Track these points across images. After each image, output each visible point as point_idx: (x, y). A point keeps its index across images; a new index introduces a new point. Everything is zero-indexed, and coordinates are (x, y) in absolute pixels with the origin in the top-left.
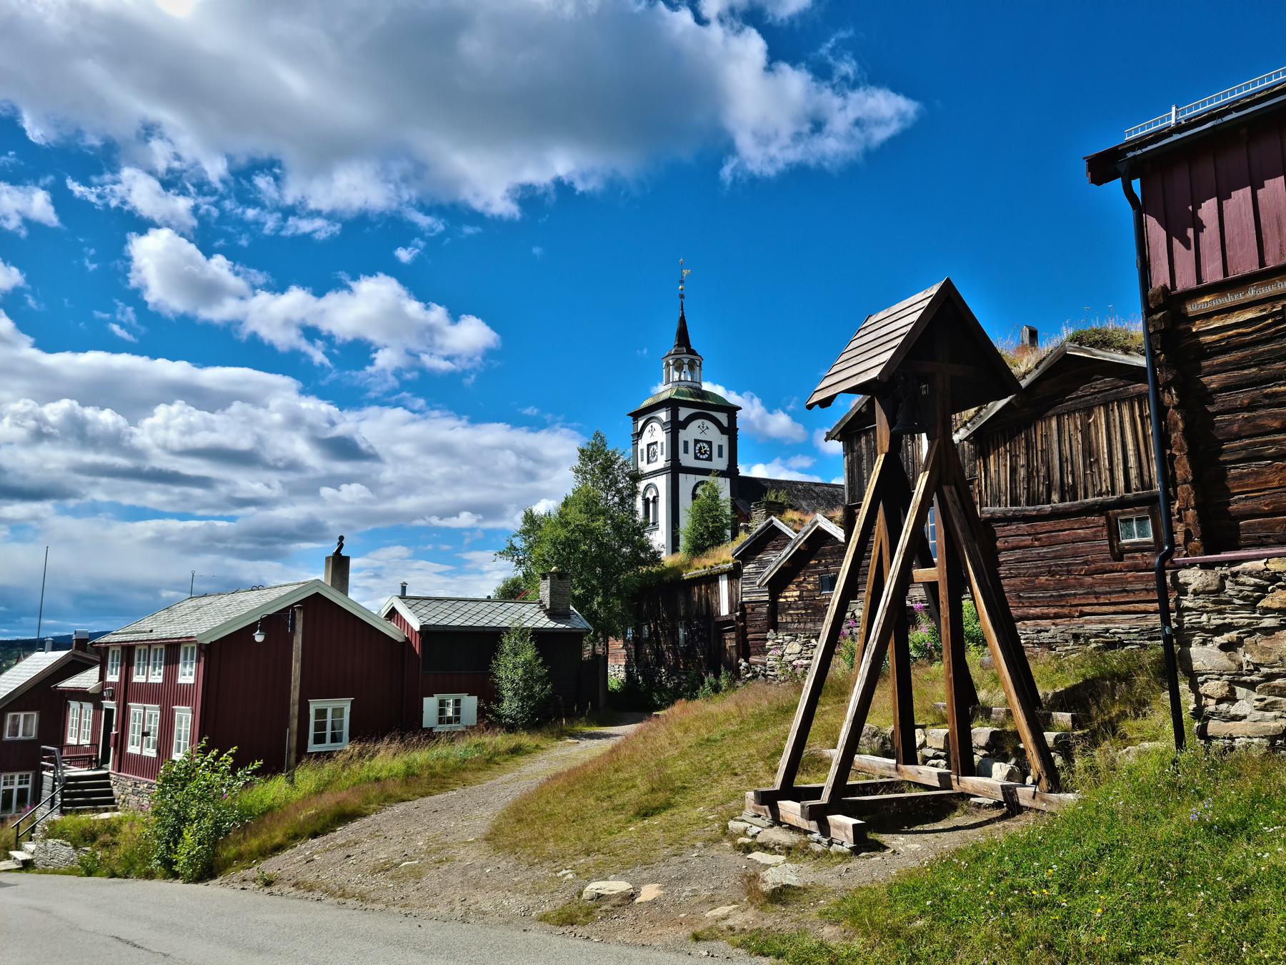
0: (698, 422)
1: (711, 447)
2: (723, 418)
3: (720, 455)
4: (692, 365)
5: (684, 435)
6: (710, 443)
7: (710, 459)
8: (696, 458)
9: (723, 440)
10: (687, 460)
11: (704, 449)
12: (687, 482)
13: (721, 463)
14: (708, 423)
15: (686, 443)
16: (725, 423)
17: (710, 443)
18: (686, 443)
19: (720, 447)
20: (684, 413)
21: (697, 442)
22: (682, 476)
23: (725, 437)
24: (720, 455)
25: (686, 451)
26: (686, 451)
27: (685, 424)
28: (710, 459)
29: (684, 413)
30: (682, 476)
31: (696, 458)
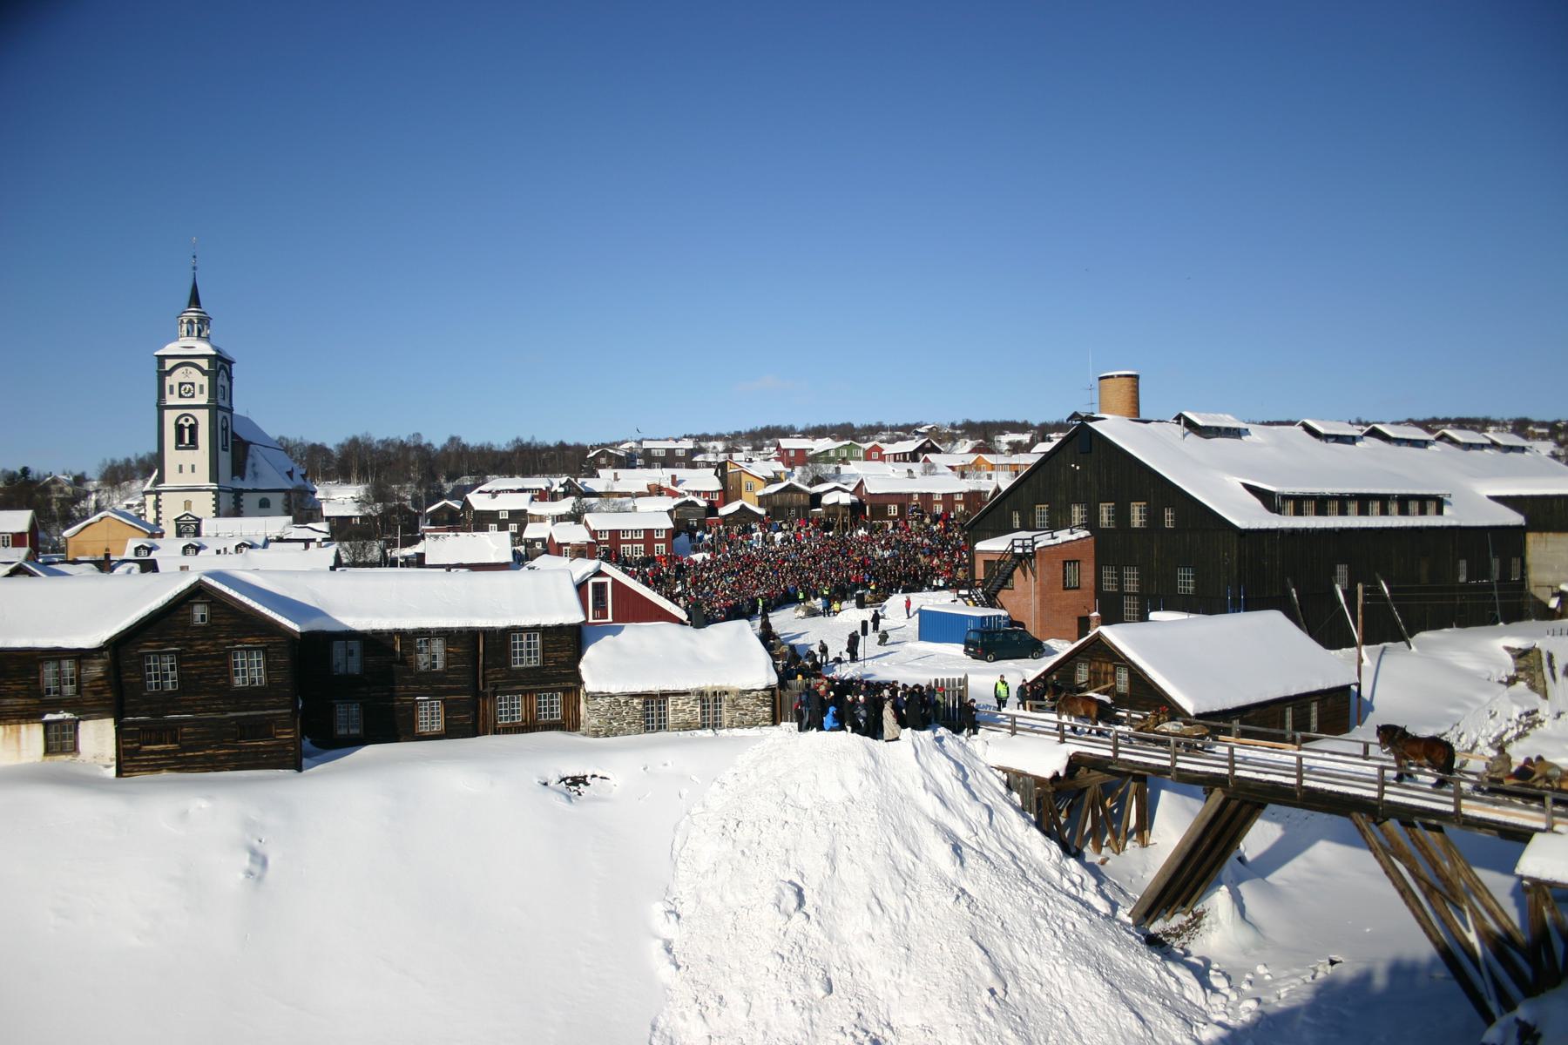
3: (201, 391)
5: (169, 381)
8: (181, 396)
9: (205, 381)
11: (185, 389)
12: (170, 417)
13: (203, 399)
14: (190, 369)
15: (171, 387)
16: (206, 368)
20: (169, 364)
21: (181, 385)
24: (201, 391)
26: (172, 392)
29: (169, 364)
31: (181, 396)
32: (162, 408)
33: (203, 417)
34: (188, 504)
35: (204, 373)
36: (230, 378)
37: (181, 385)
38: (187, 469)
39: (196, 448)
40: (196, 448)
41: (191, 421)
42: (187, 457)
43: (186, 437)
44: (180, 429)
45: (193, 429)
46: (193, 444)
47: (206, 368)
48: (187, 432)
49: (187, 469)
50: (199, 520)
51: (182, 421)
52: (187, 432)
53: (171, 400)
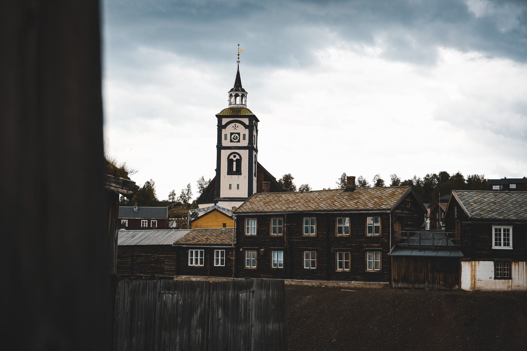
0: (233, 124)
2: (246, 121)
3: (244, 139)
4: (243, 96)
5: (224, 132)
6: (239, 134)
7: (239, 141)
8: (231, 141)
9: (247, 132)
10: (226, 143)
11: (235, 136)
12: (225, 154)
13: (245, 143)
14: (237, 124)
15: (226, 135)
17: (239, 134)
18: (226, 135)
19: (244, 135)
20: (225, 121)
21: (232, 134)
22: (223, 151)
23: (247, 130)
24: (244, 139)
25: (226, 139)
27: (225, 127)
28: (239, 141)
29: (225, 121)
30: (223, 151)
31: (231, 141)
32: (220, 147)
33: (244, 154)
35: (246, 126)
36: (257, 131)
37: (232, 134)
38: (234, 186)
39: (241, 174)
40: (241, 174)
42: (235, 178)
43: (234, 169)
44: (230, 162)
45: (239, 162)
46: (239, 172)
47: (247, 123)
48: (235, 163)
49: (234, 186)
51: (232, 157)
52: (235, 163)
53: (225, 143)
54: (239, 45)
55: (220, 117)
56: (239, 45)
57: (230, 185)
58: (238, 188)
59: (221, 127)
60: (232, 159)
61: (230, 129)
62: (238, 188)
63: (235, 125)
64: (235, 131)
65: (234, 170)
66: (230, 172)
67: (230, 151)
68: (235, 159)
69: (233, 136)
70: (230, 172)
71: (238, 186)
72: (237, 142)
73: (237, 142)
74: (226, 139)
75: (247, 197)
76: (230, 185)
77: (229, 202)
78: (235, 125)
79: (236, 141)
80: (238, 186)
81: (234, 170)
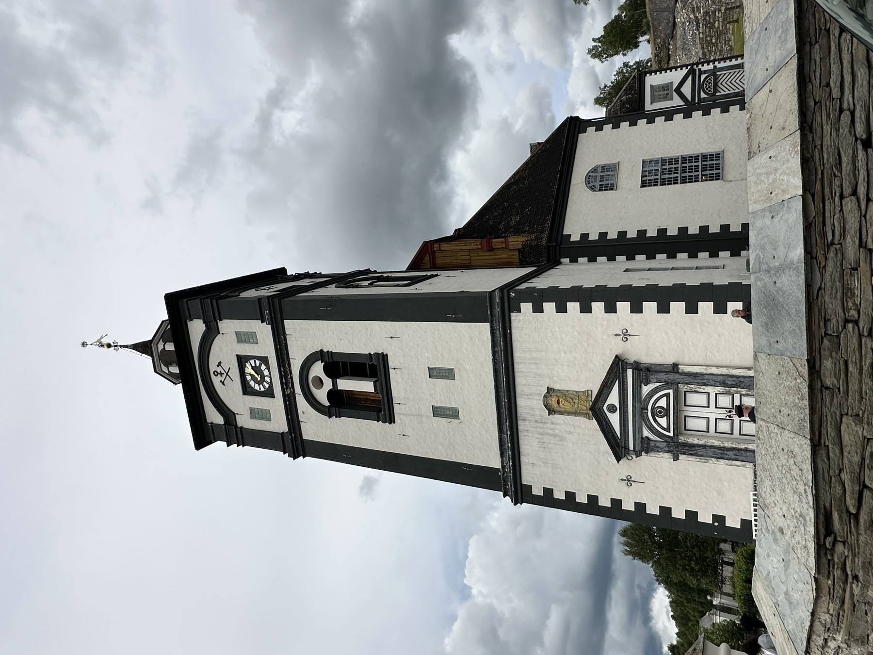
0: (216, 381)
1: (247, 358)
2: (197, 328)
5: (244, 421)
7: (265, 360)
9: (228, 327)
12: (315, 426)
14: (213, 367)
15: (255, 414)
21: (247, 390)
33: (308, 336)
34: (555, 401)
38: (441, 393)
40: (384, 357)
41: (318, 369)
46: (374, 367)
48: (344, 384)
49: (441, 393)
50: (618, 366)
51: (321, 395)
52: (344, 384)
53: (279, 424)
54: (84, 344)
55: (203, 436)
56: (84, 344)
57: (438, 412)
58: (447, 374)
59: (235, 434)
60: (333, 394)
61: (230, 392)
62: (447, 374)
63: (216, 374)
64: (235, 373)
65: (366, 386)
66: (380, 408)
67: (301, 402)
68: (328, 384)
69: (252, 383)
70: (380, 408)
71: (435, 373)
72: (268, 367)
73: (268, 367)
74: (264, 415)
75: (487, 326)
76: (438, 412)
77: (522, 426)
78: (216, 374)
79: (266, 373)
80: (435, 373)
81: (366, 386)
